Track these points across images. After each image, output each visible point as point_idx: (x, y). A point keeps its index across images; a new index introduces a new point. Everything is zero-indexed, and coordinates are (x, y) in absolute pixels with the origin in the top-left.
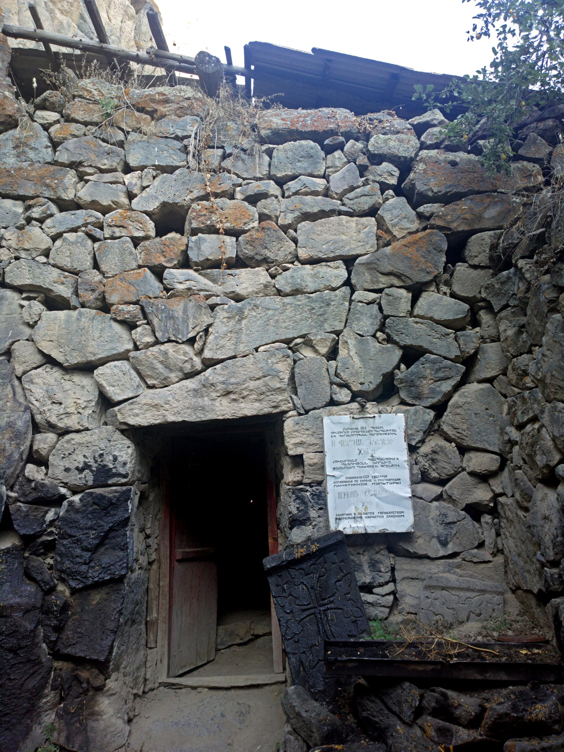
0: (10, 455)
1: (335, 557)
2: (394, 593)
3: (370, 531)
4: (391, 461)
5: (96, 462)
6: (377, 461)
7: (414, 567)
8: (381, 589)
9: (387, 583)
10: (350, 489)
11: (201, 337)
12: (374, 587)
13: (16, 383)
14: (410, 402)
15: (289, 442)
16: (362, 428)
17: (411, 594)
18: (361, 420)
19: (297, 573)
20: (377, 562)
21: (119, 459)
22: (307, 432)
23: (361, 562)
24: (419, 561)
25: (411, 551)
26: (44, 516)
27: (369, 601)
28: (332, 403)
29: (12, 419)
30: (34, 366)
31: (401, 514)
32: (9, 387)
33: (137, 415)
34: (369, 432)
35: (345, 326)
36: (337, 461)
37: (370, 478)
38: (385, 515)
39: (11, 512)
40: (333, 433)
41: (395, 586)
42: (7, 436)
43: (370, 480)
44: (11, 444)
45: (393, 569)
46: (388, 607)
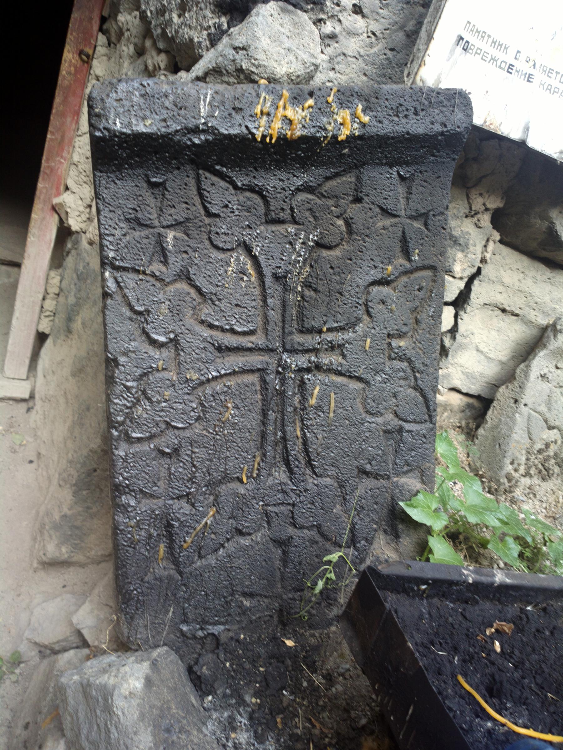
1: (401, 190)
7: (528, 284)
17: (482, 347)
19: (235, 199)
20: (455, 242)
41: (456, 316)
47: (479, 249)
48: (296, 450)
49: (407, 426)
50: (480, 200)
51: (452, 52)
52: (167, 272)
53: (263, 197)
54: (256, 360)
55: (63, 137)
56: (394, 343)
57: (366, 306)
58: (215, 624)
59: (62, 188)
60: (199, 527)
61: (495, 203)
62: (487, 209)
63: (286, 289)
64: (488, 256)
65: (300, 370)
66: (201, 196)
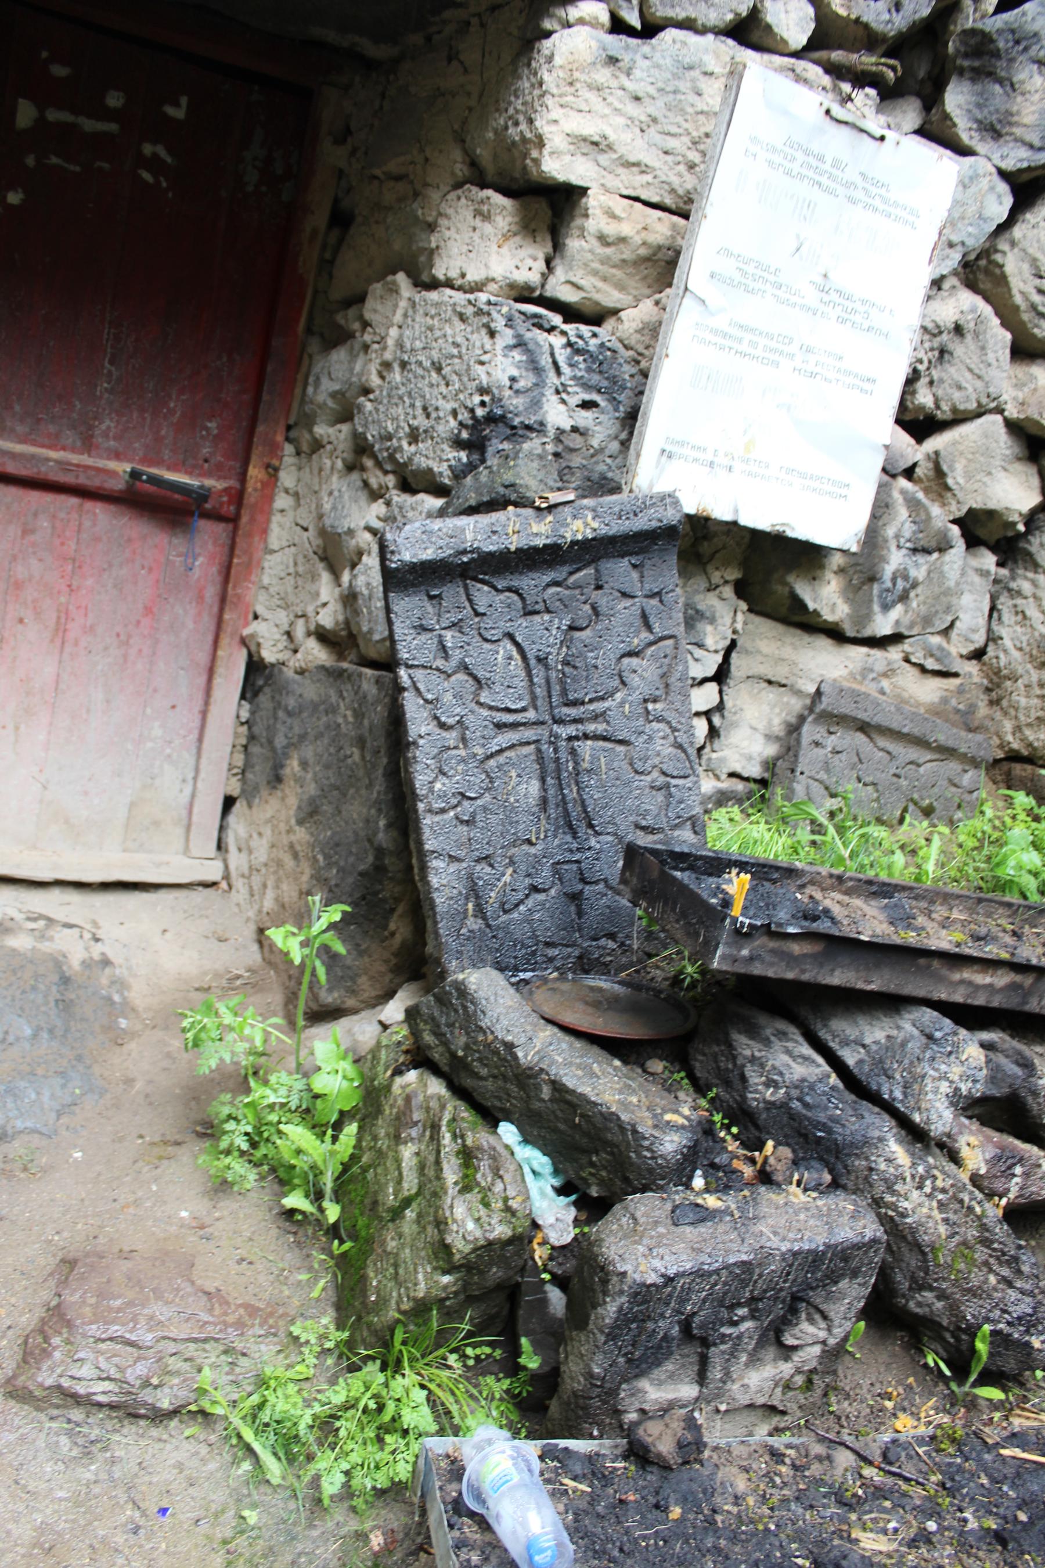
1: (635, 575)
3: (747, 520)
6: (834, 296)
7: (787, 652)
14: (965, 137)
16: (836, 164)
22: (632, 109)
24: (807, 638)
25: (811, 606)
34: (848, 185)
41: (721, 692)
47: (728, 620)
48: (575, 812)
49: (674, 782)
50: (717, 574)
51: (658, 462)
52: (449, 666)
53: (520, 595)
54: (529, 734)
55: (251, 559)
56: (650, 706)
57: (621, 677)
58: (525, 970)
59: (251, 616)
60: (500, 884)
61: (734, 574)
62: (726, 582)
63: (547, 667)
64: (739, 626)
65: (570, 739)
66: (470, 601)
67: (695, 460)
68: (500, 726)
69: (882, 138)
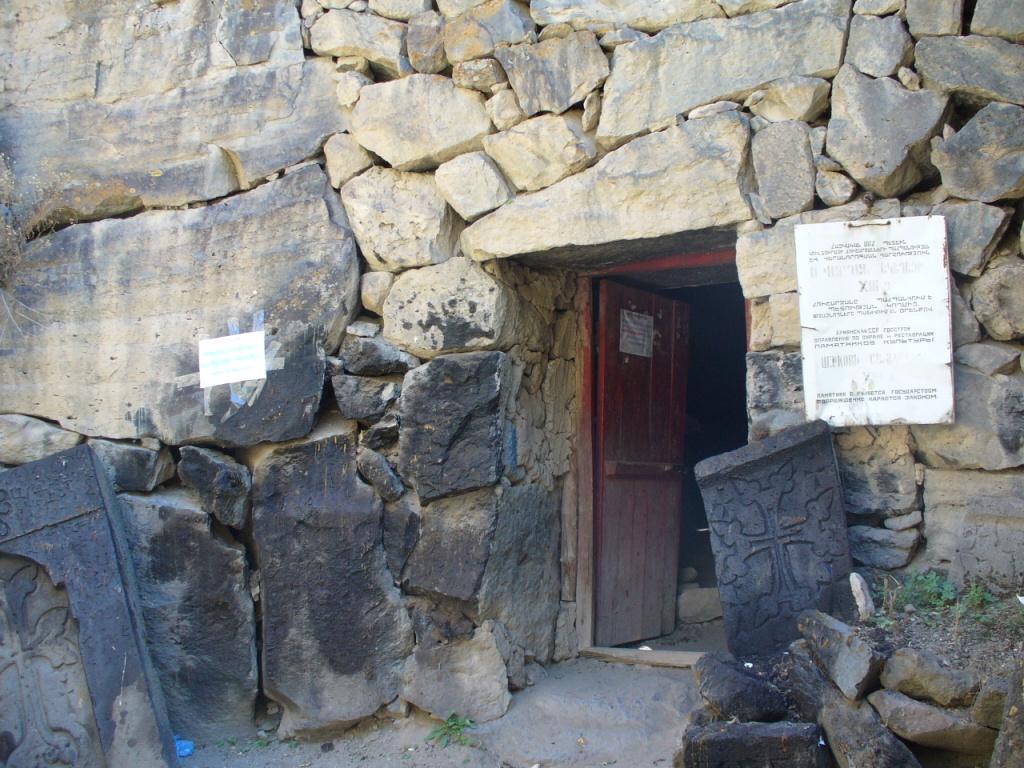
0: (326, 304)
2: (919, 526)
3: (875, 421)
4: (918, 301)
5: (446, 313)
6: (894, 301)
8: (898, 519)
9: (908, 512)
10: (844, 351)
11: (590, 102)
12: (887, 517)
13: (333, 197)
15: (745, 277)
16: (866, 244)
18: (866, 227)
20: (893, 476)
21: (479, 309)
23: (864, 476)
26: (379, 393)
27: (876, 538)
28: (818, 204)
29: (328, 252)
30: (357, 170)
31: (930, 393)
32: (323, 206)
33: (498, 238)
34: (878, 250)
35: (842, 62)
36: (820, 304)
37: (880, 332)
38: (903, 396)
39: (334, 385)
40: (813, 253)
41: (923, 516)
42: (322, 277)
43: (881, 336)
44: (327, 288)
45: (920, 489)
46: (907, 549)
67: (841, 400)
68: (751, 544)
69: (889, 223)
